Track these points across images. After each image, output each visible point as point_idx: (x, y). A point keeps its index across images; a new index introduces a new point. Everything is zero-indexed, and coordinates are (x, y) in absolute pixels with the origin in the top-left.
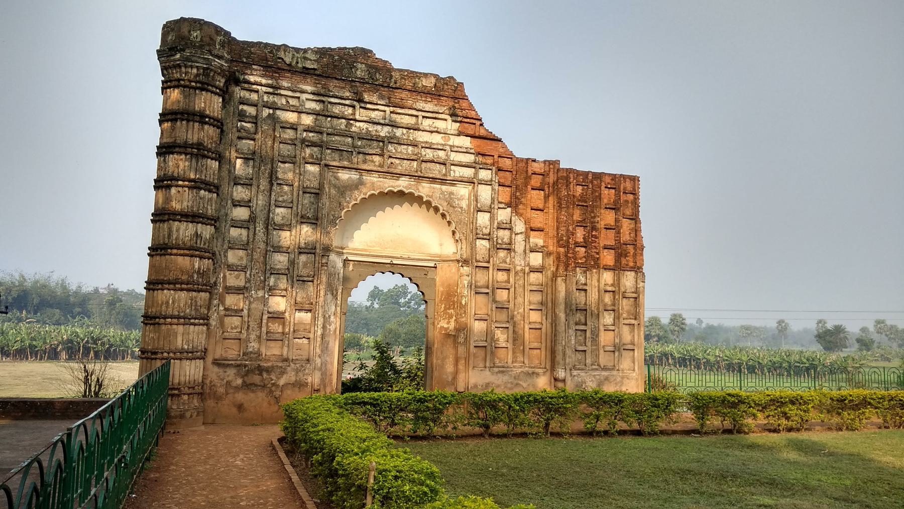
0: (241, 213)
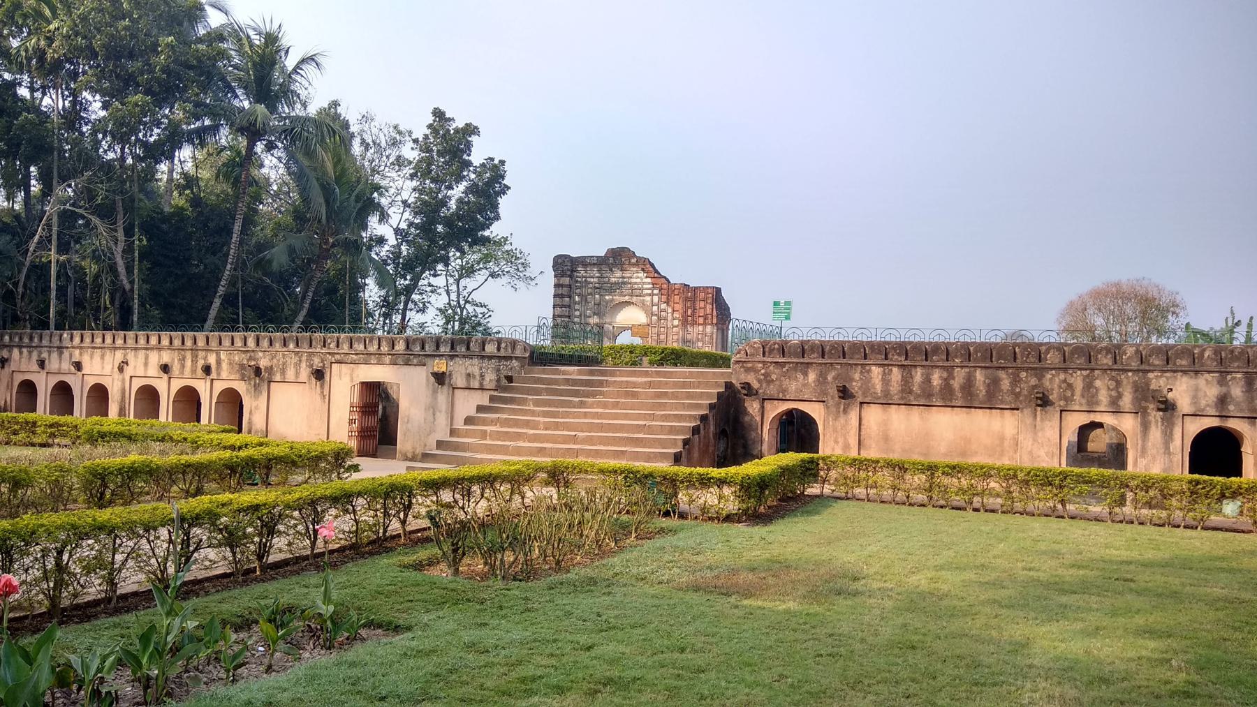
0: (577, 313)
